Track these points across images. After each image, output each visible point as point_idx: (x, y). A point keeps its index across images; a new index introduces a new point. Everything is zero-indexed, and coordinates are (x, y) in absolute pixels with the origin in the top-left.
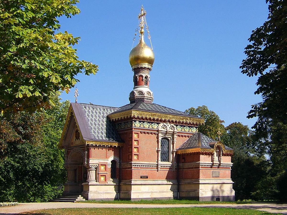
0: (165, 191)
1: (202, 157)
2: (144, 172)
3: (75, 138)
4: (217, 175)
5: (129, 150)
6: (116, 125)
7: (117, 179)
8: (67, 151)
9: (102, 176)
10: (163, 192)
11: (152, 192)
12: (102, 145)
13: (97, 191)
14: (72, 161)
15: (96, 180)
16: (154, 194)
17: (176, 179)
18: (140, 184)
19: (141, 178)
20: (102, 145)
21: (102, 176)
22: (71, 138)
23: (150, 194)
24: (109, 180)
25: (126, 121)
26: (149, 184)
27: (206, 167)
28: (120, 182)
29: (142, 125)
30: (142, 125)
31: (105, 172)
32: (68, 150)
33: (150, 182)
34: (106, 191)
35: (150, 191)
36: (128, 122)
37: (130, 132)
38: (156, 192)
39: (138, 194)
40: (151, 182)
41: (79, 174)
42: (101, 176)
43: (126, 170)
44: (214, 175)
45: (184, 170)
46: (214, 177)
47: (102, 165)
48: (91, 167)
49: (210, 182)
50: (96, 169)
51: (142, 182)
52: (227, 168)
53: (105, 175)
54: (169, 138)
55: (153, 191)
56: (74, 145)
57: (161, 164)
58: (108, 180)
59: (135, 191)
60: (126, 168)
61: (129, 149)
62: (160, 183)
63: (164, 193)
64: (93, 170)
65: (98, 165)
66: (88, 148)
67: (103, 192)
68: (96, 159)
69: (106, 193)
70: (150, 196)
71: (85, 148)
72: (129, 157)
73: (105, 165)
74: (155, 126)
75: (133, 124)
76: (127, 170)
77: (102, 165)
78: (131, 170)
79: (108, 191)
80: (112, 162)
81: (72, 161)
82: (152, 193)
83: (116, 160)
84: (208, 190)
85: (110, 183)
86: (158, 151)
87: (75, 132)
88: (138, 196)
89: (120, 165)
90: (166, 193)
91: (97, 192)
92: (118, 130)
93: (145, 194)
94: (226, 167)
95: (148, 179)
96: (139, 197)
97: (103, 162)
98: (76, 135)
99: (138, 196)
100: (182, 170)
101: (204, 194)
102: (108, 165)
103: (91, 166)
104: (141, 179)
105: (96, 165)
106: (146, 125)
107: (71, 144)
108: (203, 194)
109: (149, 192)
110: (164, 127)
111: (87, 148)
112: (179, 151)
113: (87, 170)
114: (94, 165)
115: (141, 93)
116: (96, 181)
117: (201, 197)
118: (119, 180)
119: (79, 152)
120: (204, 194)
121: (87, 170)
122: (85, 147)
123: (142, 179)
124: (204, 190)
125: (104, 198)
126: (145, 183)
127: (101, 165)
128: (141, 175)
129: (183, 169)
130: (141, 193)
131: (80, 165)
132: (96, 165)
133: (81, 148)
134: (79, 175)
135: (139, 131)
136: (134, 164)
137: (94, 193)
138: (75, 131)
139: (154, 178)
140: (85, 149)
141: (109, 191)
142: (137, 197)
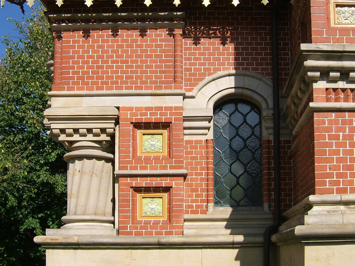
9: (147, 190)
31: (165, 168)
53: (164, 182)
58: (186, 216)
64: (81, 158)
73: (166, 125)
102: (187, 124)
103: (63, 131)
105: (96, 126)
114: (82, 126)
127: (138, 125)
132: (96, 126)
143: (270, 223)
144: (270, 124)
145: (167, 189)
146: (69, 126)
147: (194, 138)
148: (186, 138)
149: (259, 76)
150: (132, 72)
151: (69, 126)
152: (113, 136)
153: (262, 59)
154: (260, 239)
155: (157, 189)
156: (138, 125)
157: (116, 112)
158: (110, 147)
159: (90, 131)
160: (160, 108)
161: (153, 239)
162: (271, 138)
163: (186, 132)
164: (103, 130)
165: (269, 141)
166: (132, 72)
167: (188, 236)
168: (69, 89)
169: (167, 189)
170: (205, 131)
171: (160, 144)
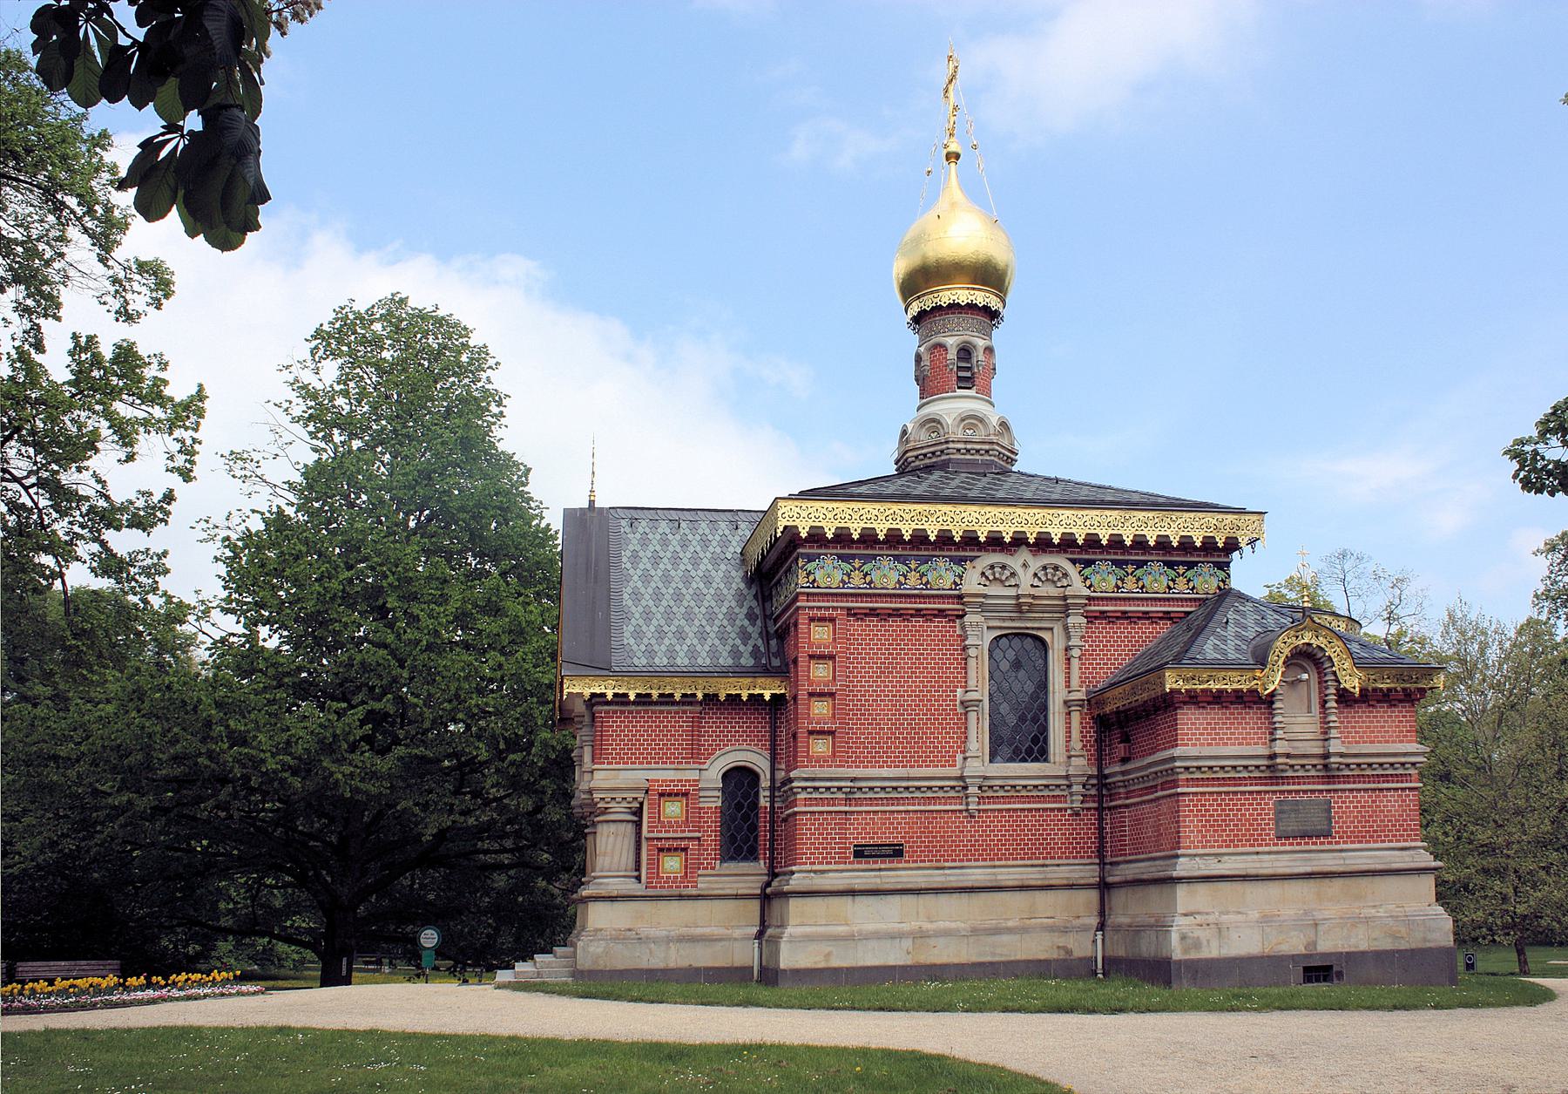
0: (1010, 924)
1: (1190, 721)
2: (869, 827)
4: (1316, 821)
7: (762, 862)
9: (669, 850)
10: (996, 931)
11: (920, 936)
12: (655, 694)
13: (630, 930)
15: (636, 874)
16: (932, 942)
18: (841, 888)
19: (859, 853)
20: (655, 694)
21: (669, 850)
23: (907, 944)
24: (713, 868)
26: (899, 887)
27: (1223, 776)
29: (913, 577)
30: (857, 575)
33: (909, 876)
34: (684, 931)
35: (906, 927)
38: (946, 933)
39: (825, 948)
40: (916, 876)
42: (661, 850)
44: (1292, 827)
46: (1287, 838)
47: (670, 795)
48: (606, 808)
49: (1258, 865)
51: (858, 877)
52: (1386, 778)
54: (1040, 634)
55: (927, 926)
57: (985, 778)
58: (700, 872)
59: (808, 930)
62: (977, 880)
63: (1005, 938)
65: (640, 795)
67: (664, 933)
68: (629, 766)
69: (682, 939)
70: (908, 953)
73: (686, 794)
74: (942, 575)
75: (802, 574)
77: (670, 795)
79: (699, 931)
80: (725, 776)
82: (919, 941)
84: (1240, 917)
85: (713, 889)
88: (828, 955)
90: (1018, 937)
91: (629, 933)
93: (873, 944)
94: (1379, 773)
95: (906, 861)
96: (835, 963)
97: (674, 781)
99: (828, 955)
101: (1208, 941)
103: (603, 799)
104: (861, 863)
105: (630, 795)
106: (887, 574)
108: (1205, 943)
109: (900, 936)
110: (997, 575)
114: (619, 796)
117: (1186, 961)
120: (1208, 941)
123: (864, 860)
124: (1211, 919)
125: (672, 965)
126: (878, 880)
130: (850, 938)
132: (630, 795)
135: (842, 608)
136: (806, 779)
137: (615, 939)
139: (938, 855)
141: (707, 931)
142: (815, 963)
143: (766, 878)
144: (768, 793)
145: (685, 850)
146: (608, 795)
147: (706, 805)
148: (701, 805)
149: (759, 751)
150: (659, 749)
151: (608, 795)
152: (642, 804)
153: (762, 736)
154: (759, 892)
155: (676, 849)
156: (661, 795)
157: (647, 785)
158: (638, 812)
159: (624, 799)
160: (681, 781)
161: (675, 891)
162: (768, 805)
163: (702, 800)
164: (635, 799)
165: (766, 808)
166: (659, 749)
167: (701, 889)
168: (608, 763)
169: (685, 850)
170: (716, 799)
171: (678, 811)
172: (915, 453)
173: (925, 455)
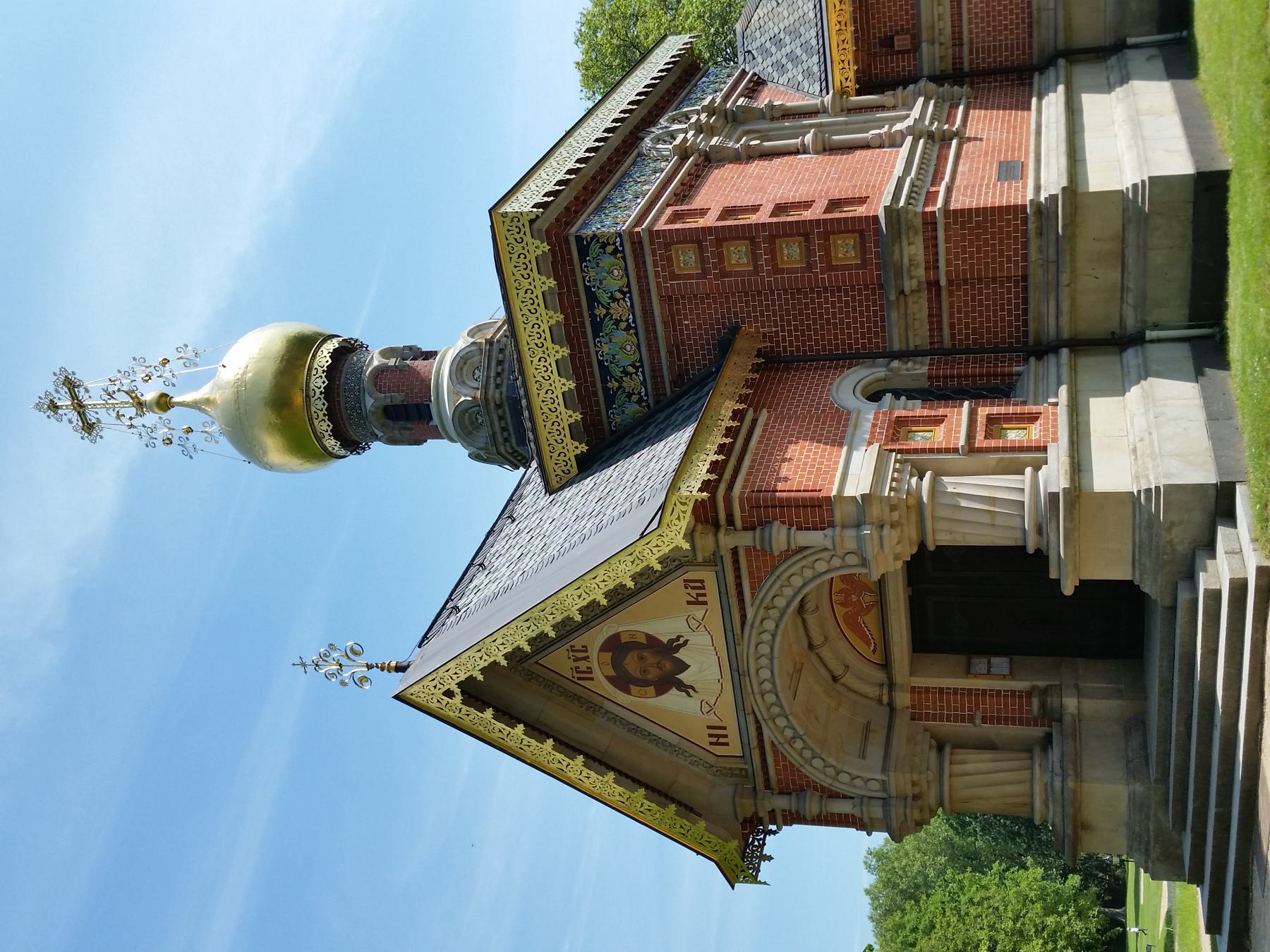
3: (673, 698)
5: (790, 271)
6: (618, 419)
8: (781, 793)
14: (863, 758)
15: (1029, 470)
17: (1031, 77)
22: (674, 739)
25: (586, 314)
28: (1043, 350)
32: (768, 786)
36: (587, 289)
37: (655, 266)
41: (979, 715)
43: (943, 282)
45: (970, 31)
50: (928, 474)
56: (727, 714)
60: (933, 285)
61: (782, 271)
66: (738, 523)
71: (742, 553)
72: (849, 267)
76: (948, 273)
78: (947, 228)
81: (863, 758)
83: (867, 379)
86: (820, 148)
87: (628, 692)
89: (905, 355)
92: (651, 401)
98: (643, 683)
100: (966, 48)
107: (720, 750)
111: (745, 529)
112: (838, 84)
113: (931, 547)
115: (462, 362)
116: (1037, 468)
118: (1032, 360)
119: (778, 639)
121: (931, 547)
122: (735, 551)
128: (994, 177)
129: (961, 45)
131: (903, 699)
133: (750, 615)
134: (984, 720)
138: (621, 697)
140: (747, 549)
172: (492, 386)
173: (498, 375)
